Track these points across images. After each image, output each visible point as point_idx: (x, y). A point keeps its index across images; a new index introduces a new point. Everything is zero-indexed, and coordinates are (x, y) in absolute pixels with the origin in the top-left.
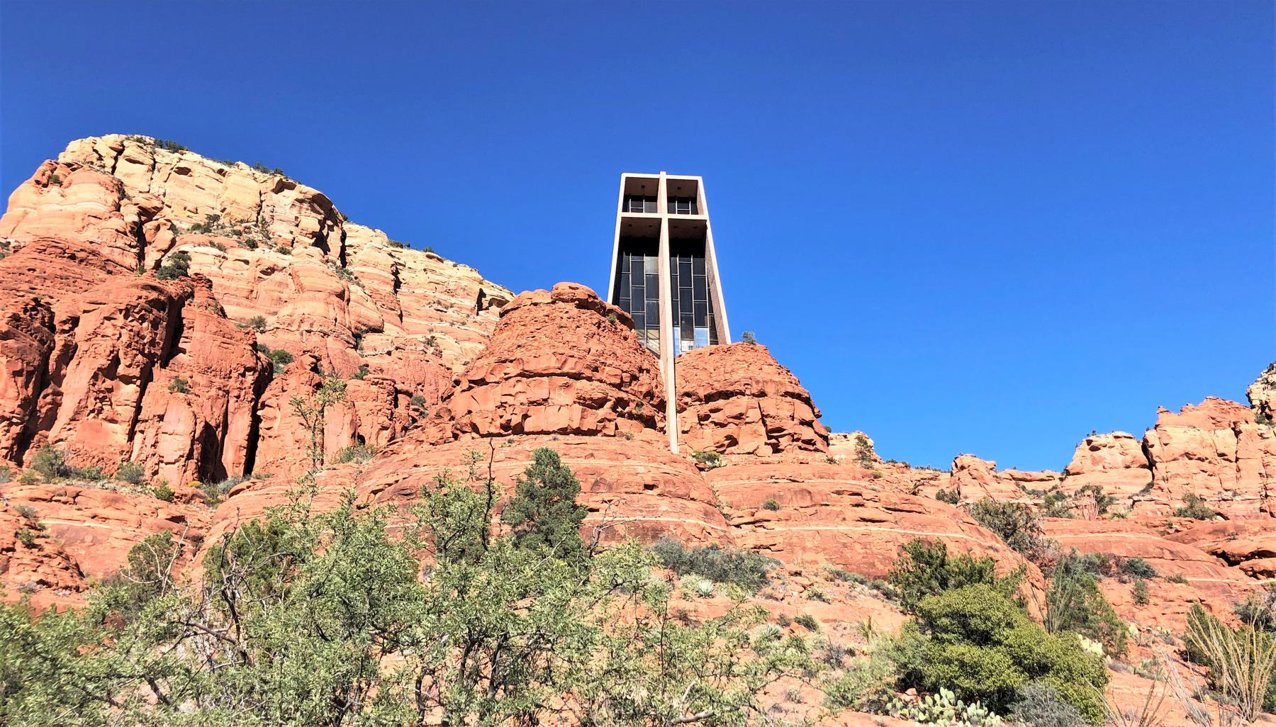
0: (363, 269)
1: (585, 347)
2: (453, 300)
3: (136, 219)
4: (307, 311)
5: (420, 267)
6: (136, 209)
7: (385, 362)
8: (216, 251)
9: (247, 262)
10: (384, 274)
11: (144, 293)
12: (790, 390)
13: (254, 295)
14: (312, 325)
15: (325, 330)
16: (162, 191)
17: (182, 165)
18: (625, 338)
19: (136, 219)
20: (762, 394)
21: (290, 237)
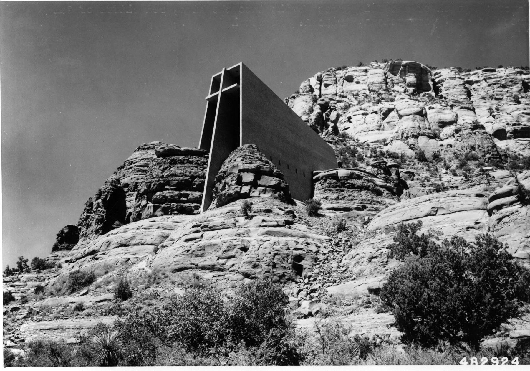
0: (448, 92)
1: (160, 175)
2: (506, 89)
3: (319, 111)
4: (403, 127)
5: (481, 78)
6: (318, 106)
7: (452, 141)
9: (376, 112)
10: (459, 90)
12: (241, 167)
13: (382, 127)
14: (407, 134)
15: (415, 134)
16: (341, 90)
17: (347, 75)
18: (191, 163)
19: (319, 111)
20: (230, 173)
21: (403, 90)
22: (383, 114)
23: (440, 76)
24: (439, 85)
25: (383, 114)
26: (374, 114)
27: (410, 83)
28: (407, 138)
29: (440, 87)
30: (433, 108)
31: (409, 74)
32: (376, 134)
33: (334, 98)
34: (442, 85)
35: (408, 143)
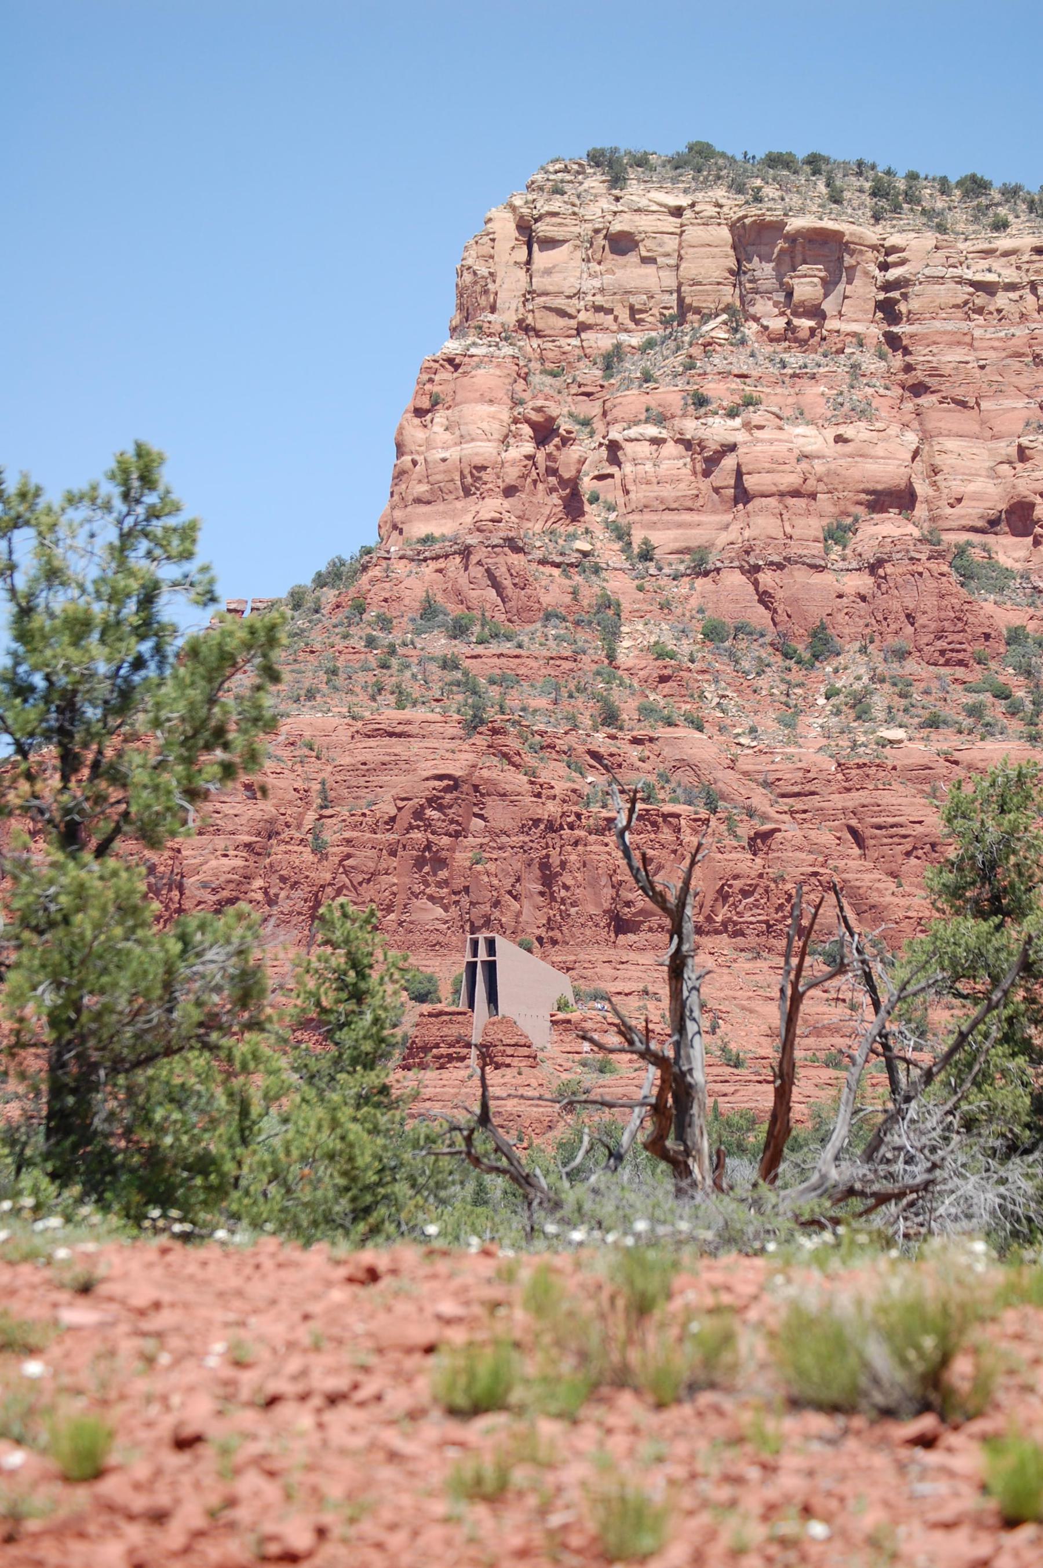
8: (652, 431)
9: (688, 444)
11: (436, 783)
22: (706, 460)
23: (903, 262)
24: (895, 294)
25: (706, 460)
26: (681, 447)
27: (802, 303)
28: (757, 569)
29: (897, 301)
30: (846, 441)
31: (803, 268)
32: (680, 525)
33: (572, 311)
34: (905, 296)
35: (756, 583)
